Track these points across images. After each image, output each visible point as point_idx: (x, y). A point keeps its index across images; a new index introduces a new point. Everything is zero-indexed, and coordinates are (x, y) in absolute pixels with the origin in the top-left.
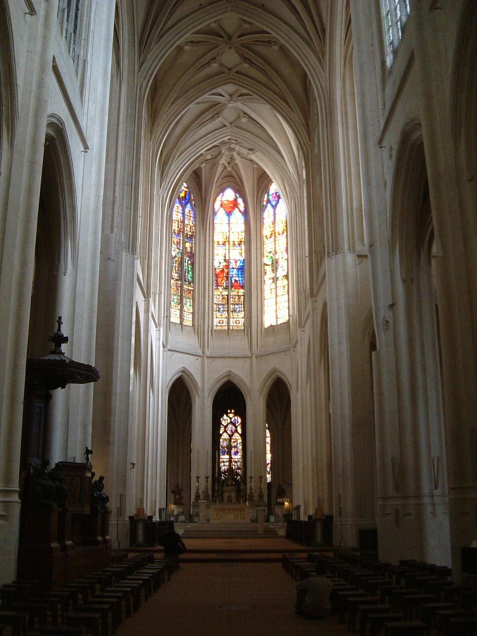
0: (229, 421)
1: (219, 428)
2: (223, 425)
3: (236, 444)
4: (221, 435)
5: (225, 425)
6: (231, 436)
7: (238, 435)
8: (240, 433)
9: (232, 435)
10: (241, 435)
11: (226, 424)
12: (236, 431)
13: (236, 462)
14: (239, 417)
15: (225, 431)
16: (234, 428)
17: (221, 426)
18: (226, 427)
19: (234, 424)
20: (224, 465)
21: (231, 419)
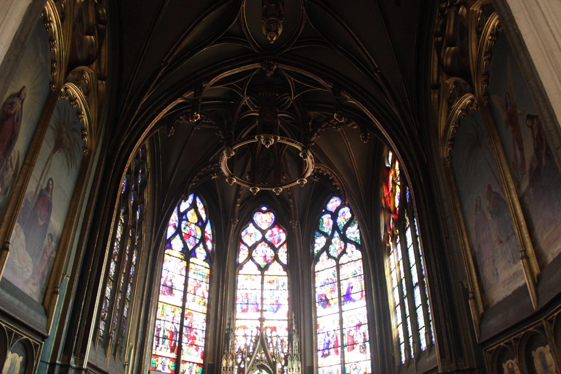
0: (259, 236)
1: (237, 251)
2: (246, 245)
3: (274, 286)
4: (241, 266)
5: (250, 245)
6: (262, 270)
7: (281, 267)
8: (285, 261)
9: (267, 267)
10: (285, 268)
11: (254, 242)
12: (276, 258)
13: (274, 329)
14: (281, 231)
15: (250, 257)
16: (270, 253)
17: (242, 246)
18: (252, 249)
19: (271, 245)
20: (245, 336)
21: (263, 232)
